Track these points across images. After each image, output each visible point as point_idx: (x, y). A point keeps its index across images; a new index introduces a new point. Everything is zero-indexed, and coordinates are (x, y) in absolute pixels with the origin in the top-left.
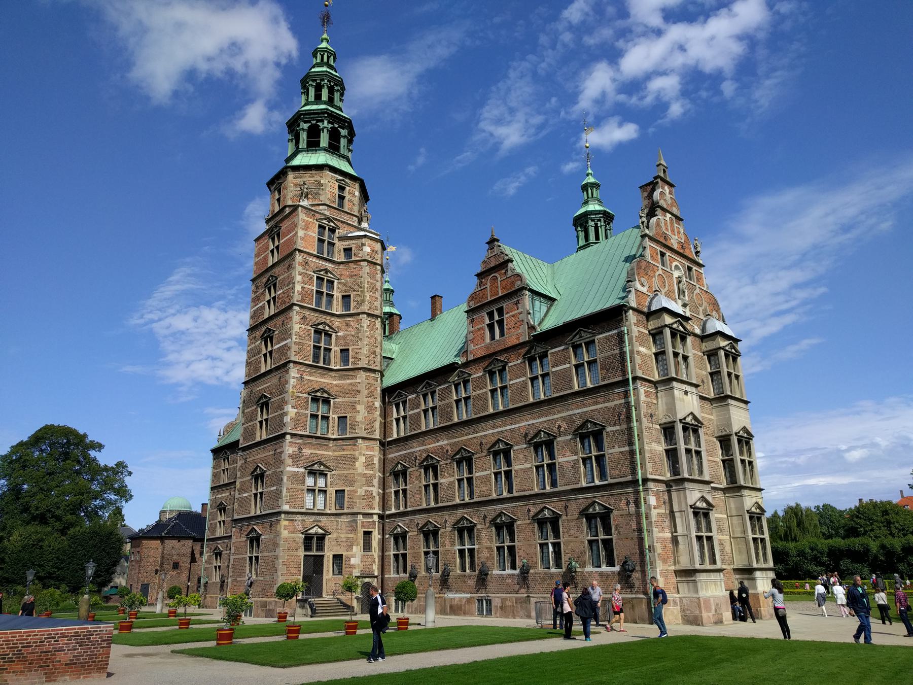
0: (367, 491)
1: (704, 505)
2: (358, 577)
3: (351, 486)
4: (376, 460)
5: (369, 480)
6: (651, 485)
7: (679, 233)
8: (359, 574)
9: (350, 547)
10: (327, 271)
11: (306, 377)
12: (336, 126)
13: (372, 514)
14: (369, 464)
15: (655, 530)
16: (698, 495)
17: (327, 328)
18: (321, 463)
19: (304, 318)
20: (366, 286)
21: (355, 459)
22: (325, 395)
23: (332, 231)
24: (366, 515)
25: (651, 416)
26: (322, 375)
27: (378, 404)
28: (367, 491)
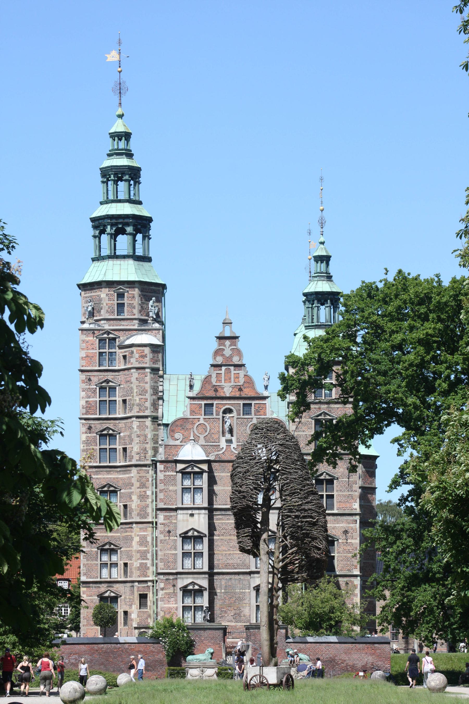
0: (141, 564)
1: (196, 587)
2: (135, 628)
3: (131, 560)
4: (149, 539)
5: (143, 555)
6: (162, 577)
7: (237, 377)
8: (136, 626)
9: (131, 605)
10: (107, 381)
11: (93, 476)
12: (120, 226)
13: (146, 582)
14: (143, 542)
15: (159, 603)
16: (190, 581)
17: (111, 432)
18: (111, 544)
19: (90, 428)
20: (135, 391)
21: (132, 539)
22: (112, 489)
23: (114, 339)
24: (139, 582)
25: (169, 532)
26: (108, 472)
27: (149, 493)
28: (141, 564)
